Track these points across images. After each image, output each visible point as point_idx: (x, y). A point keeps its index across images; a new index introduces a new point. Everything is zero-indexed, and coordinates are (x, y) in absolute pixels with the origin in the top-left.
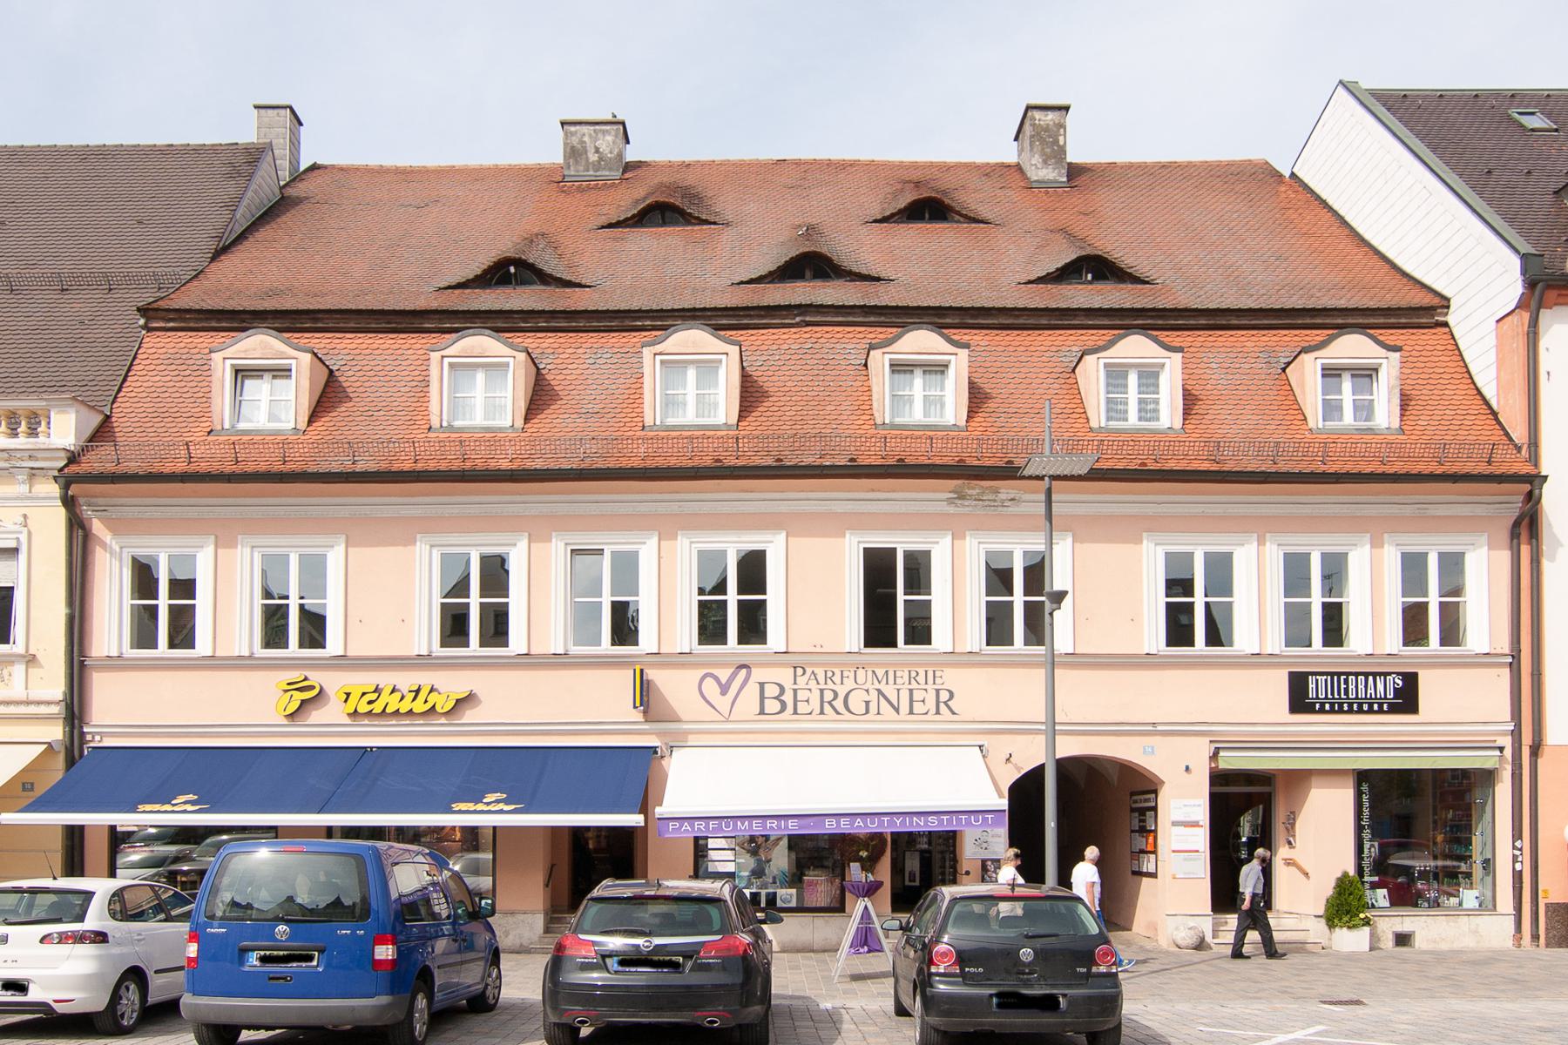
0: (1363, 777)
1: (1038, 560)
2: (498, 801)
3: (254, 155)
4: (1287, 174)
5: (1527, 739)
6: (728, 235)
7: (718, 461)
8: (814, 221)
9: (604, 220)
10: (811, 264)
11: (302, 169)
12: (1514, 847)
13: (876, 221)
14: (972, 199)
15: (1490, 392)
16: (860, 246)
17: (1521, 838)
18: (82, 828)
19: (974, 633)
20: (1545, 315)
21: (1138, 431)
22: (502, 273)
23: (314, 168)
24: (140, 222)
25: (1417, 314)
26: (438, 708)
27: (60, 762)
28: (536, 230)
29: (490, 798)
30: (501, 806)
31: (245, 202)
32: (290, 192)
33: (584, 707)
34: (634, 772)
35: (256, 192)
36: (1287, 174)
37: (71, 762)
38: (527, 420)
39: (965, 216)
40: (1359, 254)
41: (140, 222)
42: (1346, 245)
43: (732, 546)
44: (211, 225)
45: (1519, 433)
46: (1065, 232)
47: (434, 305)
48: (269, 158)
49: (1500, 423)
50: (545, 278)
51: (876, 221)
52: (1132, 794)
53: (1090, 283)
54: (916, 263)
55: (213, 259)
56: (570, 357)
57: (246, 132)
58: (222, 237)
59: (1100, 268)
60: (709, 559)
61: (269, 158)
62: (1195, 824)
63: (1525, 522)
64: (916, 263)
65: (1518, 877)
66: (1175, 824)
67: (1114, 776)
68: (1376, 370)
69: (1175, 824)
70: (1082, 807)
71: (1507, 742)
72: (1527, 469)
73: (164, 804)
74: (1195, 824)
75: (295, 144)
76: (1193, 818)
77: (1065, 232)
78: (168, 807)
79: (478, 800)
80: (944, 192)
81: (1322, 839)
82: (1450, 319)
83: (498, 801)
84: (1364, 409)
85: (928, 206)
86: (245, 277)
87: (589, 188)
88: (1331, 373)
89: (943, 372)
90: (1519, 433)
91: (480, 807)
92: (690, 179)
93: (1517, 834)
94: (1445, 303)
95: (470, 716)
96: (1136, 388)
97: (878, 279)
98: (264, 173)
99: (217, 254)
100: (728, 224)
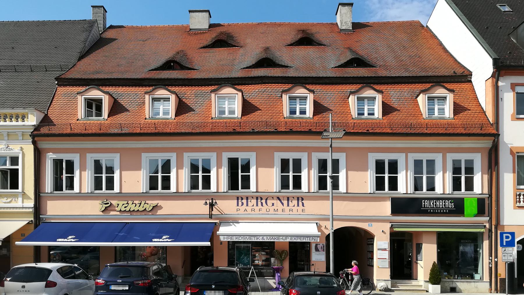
0: (439, 234)
1: (246, 162)
2: (166, 238)
3: (92, 24)
4: (425, 26)
5: (494, 223)
6: (242, 51)
7: (234, 130)
8: (268, 45)
9: (202, 45)
10: (265, 62)
11: (107, 27)
12: (489, 259)
13: (288, 45)
14: (321, 36)
15: (483, 105)
16: (284, 55)
17: (492, 257)
18: (40, 247)
19: (314, 186)
20: (501, 78)
21: (367, 119)
22: (168, 65)
23: (111, 27)
24: (56, 47)
25: (463, 77)
26: (147, 209)
27: (33, 226)
28: (180, 49)
29: (164, 237)
30: (167, 240)
31: (89, 40)
32: (105, 36)
33: (195, 209)
34: (209, 230)
35: (92, 37)
36: (425, 26)
37: (36, 226)
38: (176, 116)
39: (317, 43)
40: (445, 56)
41: (56, 47)
42: (441, 52)
43: (161, 157)
44: (78, 49)
45: (491, 119)
46: (350, 49)
47: (147, 76)
48: (96, 25)
49: (486, 116)
50: (183, 68)
51: (288, 45)
52: (368, 239)
53: (355, 67)
54: (299, 60)
55: (79, 60)
56: (189, 94)
57: (88, 15)
58: (84, 51)
59: (357, 62)
60: (153, 162)
61: (96, 25)
62: (385, 250)
63: (493, 149)
64: (299, 60)
65: (491, 269)
66: (379, 249)
67: (363, 234)
68: (446, 98)
69: (379, 249)
70: (351, 244)
71: (487, 226)
72: (494, 132)
73: (65, 239)
74: (385, 250)
75: (104, 19)
76: (383, 247)
77: (350, 49)
78: (66, 240)
79: (160, 238)
80: (312, 34)
81: (428, 256)
82: (472, 80)
83: (166, 238)
84: (442, 111)
85: (306, 39)
86: (89, 67)
87: (198, 34)
88: (431, 99)
89: (306, 100)
90: (491, 119)
91: (161, 240)
92: (231, 30)
93: (490, 255)
94: (471, 74)
95: (160, 212)
96: (371, 105)
97: (287, 67)
98: (95, 31)
99: (81, 58)
100: (241, 47)
